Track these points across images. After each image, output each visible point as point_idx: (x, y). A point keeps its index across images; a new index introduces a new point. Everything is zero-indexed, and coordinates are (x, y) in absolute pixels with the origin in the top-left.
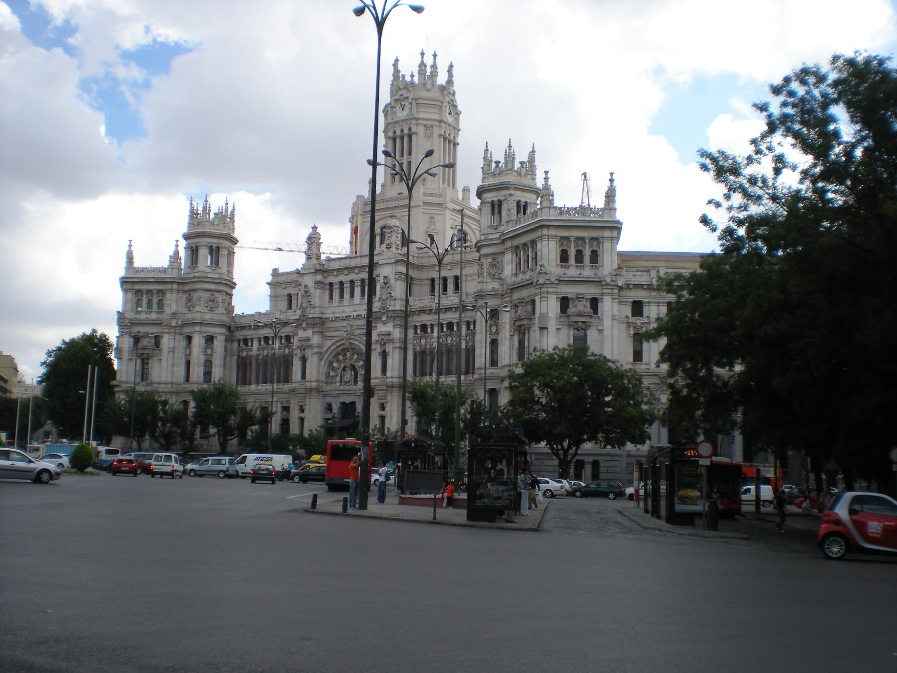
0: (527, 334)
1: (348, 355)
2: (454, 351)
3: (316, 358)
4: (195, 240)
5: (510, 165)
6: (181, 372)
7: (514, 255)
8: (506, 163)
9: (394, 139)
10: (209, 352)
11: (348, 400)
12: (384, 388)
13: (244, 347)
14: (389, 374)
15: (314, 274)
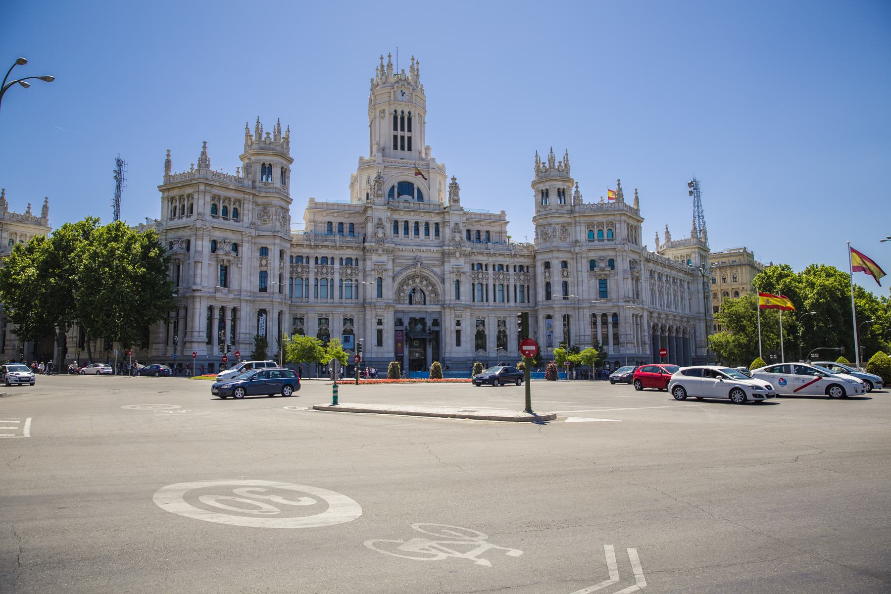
0: (608, 281)
1: (418, 280)
2: (506, 285)
3: (391, 280)
4: (267, 158)
5: (552, 164)
6: (256, 281)
7: (586, 228)
8: (566, 165)
9: (395, 118)
10: (282, 264)
11: (418, 316)
12: (462, 309)
13: (300, 264)
14: (462, 298)
15: (385, 211)
